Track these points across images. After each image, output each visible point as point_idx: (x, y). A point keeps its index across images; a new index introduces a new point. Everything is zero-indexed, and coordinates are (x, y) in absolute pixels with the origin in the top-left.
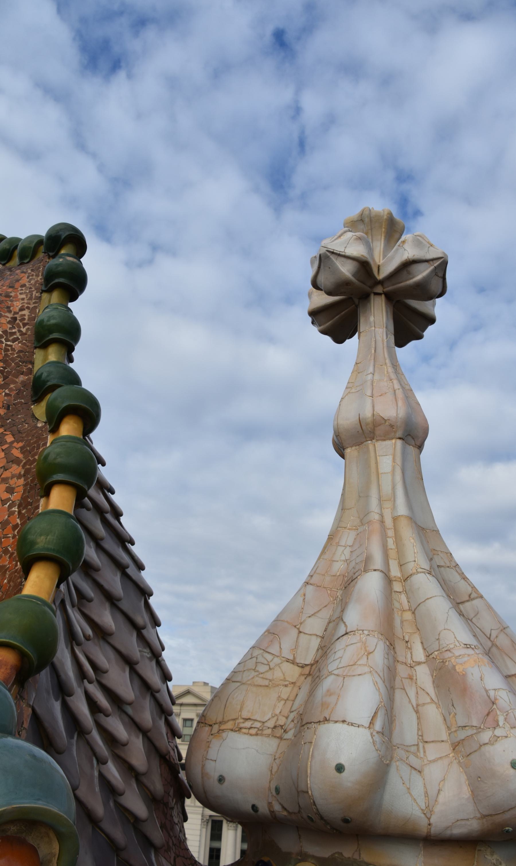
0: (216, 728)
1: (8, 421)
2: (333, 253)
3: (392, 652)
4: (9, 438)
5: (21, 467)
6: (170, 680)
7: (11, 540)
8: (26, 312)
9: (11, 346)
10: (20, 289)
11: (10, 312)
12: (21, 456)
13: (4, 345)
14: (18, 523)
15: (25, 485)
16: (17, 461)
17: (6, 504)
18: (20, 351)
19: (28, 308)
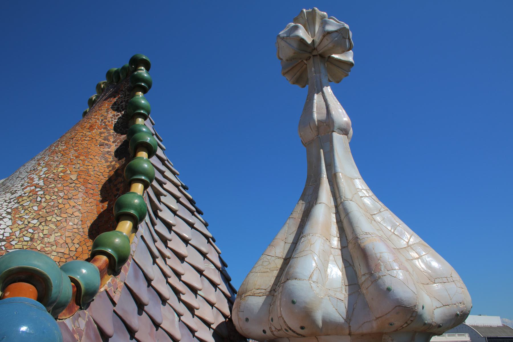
0: (244, 295)
3: (328, 243)
6: (230, 280)
8: (124, 103)
18: (122, 123)
19: (124, 101)
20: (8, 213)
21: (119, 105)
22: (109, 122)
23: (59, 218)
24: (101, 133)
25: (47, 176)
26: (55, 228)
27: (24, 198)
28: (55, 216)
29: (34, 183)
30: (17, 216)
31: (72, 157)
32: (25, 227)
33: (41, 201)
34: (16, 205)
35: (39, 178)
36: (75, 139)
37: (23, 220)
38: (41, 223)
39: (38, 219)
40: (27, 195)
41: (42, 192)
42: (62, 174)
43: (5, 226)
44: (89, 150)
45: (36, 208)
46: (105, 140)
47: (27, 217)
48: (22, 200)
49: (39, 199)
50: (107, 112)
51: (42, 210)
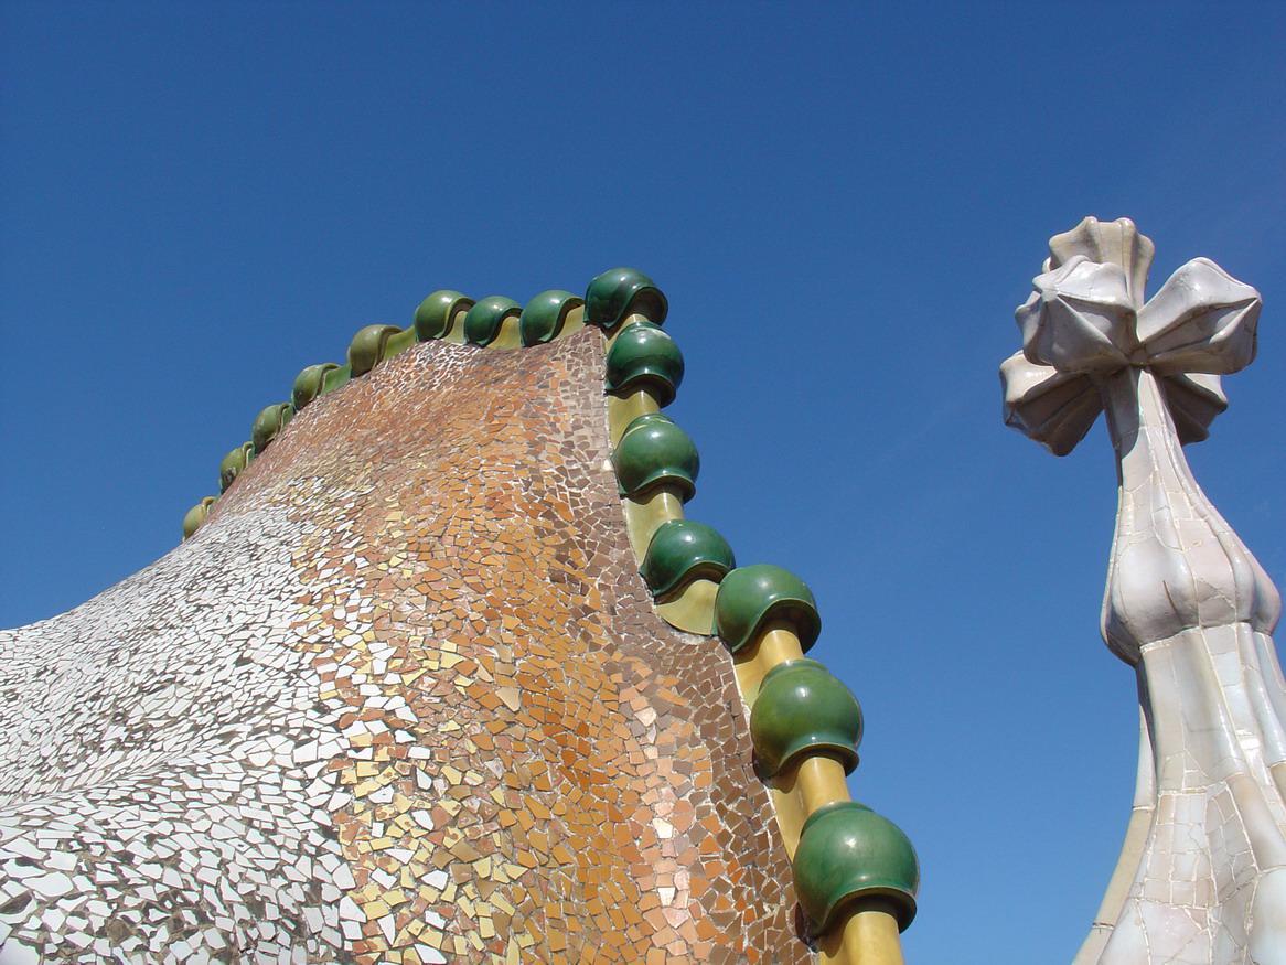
1: (623, 637)
2: (1069, 300)
4: (643, 670)
5: (691, 724)
7: (725, 864)
9: (579, 495)
10: (560, 389)
11: (558, 432)
12: (686, 703)
13: (568, 494)
14: (725, 831)
15: (715, 756)
16: (681, 713)
17: (683, 795)
18: (597, 505)
19: (588, 423)
20: (328, 833)
21: (568, 434)
22: (553, 492)
23: (517, 872)
24: (539, 531)
25: (408, 679)
26: (511, 910)
27: (365, 769)
28: (498, 859)
29: (368, 704)
30: (364, 847)
31: (473, 616)
32: (409, 903)
33: (432, 789)
34: (340, 799)
35: (384, 688)
36: (449, 540)
37: (393, 867)
38: (460, 886)
39: (445, 869)
40: (367, 753)
41: (424, 753)
42: (463, 681)
43: (338, 894)
44: (525, 595)
45: (424, 819)
46: (561, 559)
47: (405, 856)
48: (361, 779)
49: (424, 781)
50: (536, 454)
51: (452, 831)
